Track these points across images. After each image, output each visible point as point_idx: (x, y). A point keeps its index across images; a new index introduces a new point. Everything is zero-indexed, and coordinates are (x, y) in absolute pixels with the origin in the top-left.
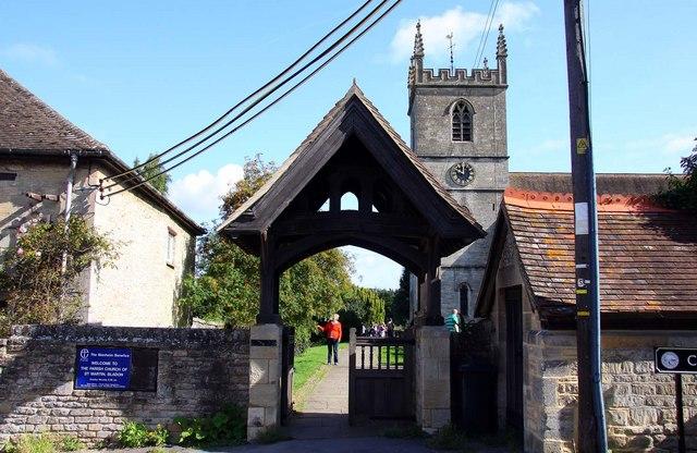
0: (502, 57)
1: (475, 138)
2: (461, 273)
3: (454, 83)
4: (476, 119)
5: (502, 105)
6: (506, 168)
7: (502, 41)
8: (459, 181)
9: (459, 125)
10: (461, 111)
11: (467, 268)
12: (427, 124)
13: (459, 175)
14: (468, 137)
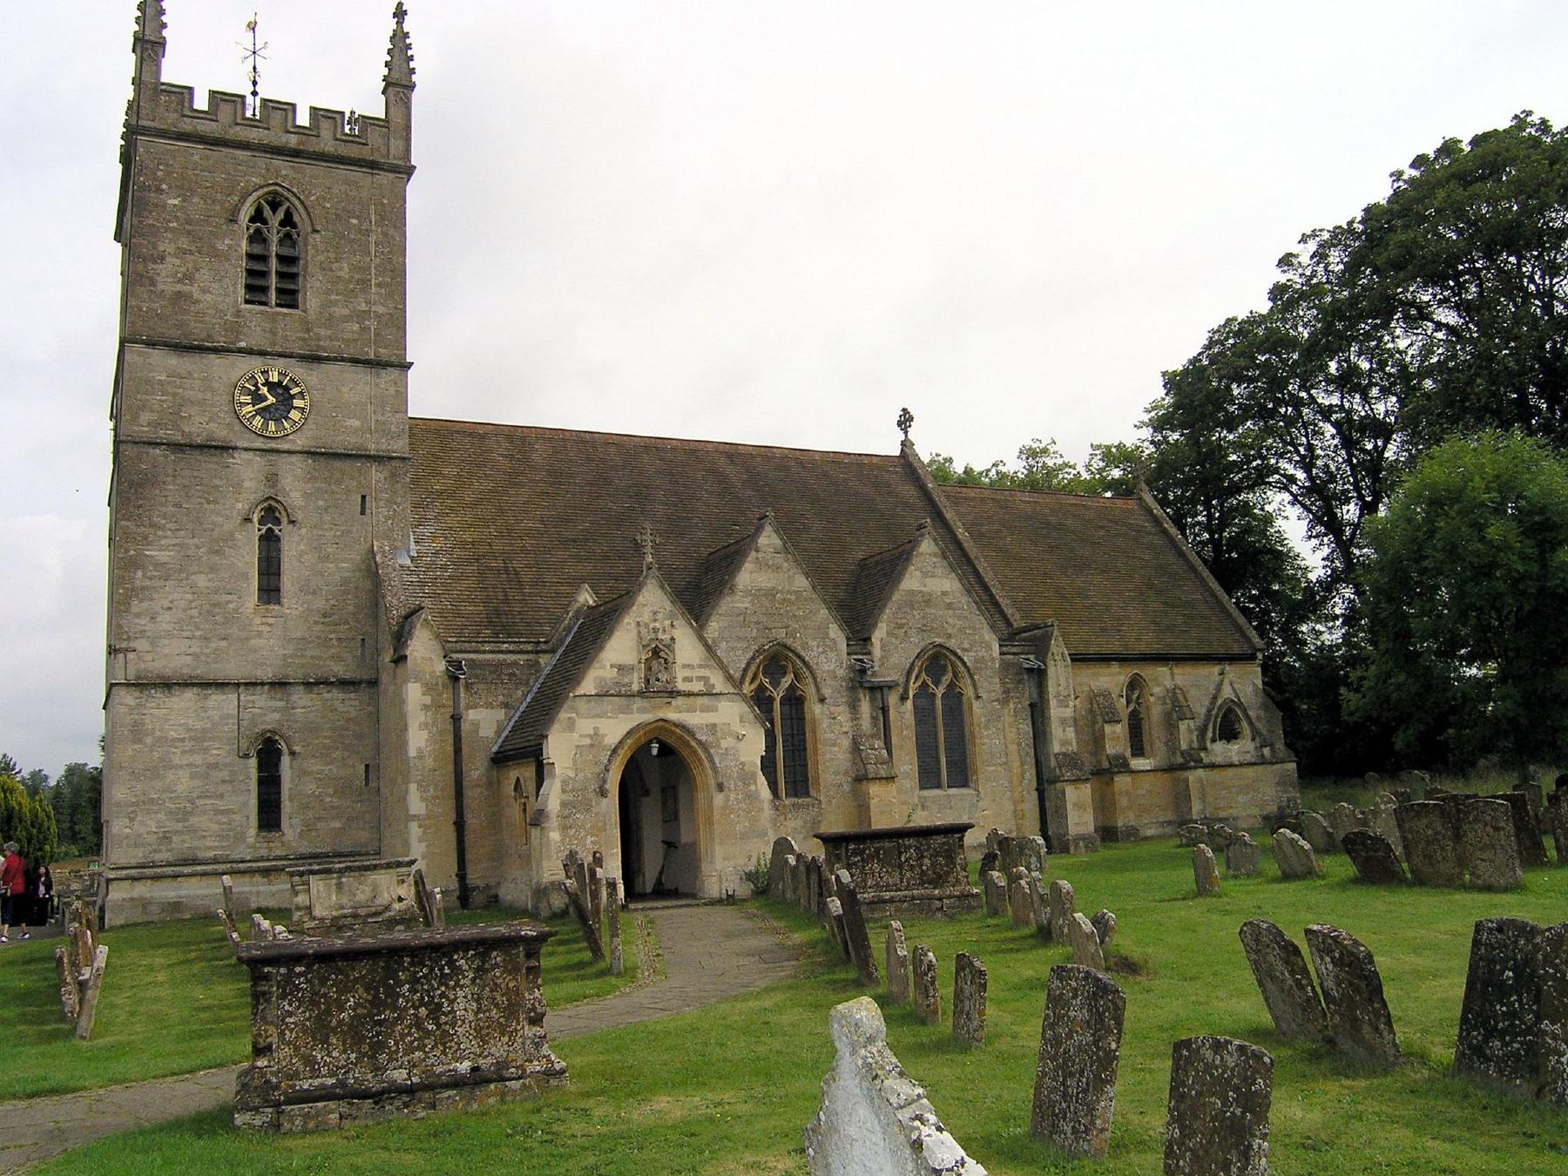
0: (399, 84)
3: (253, 135)
4: (314, 251)
5: (394, 218)
6: (402, 396)
7: (400, 43)
8: (258, 422)
9: (263, 258)
10: (275, 220)
11: (280, 685)
12: (165, 246)
14: (289, 298)
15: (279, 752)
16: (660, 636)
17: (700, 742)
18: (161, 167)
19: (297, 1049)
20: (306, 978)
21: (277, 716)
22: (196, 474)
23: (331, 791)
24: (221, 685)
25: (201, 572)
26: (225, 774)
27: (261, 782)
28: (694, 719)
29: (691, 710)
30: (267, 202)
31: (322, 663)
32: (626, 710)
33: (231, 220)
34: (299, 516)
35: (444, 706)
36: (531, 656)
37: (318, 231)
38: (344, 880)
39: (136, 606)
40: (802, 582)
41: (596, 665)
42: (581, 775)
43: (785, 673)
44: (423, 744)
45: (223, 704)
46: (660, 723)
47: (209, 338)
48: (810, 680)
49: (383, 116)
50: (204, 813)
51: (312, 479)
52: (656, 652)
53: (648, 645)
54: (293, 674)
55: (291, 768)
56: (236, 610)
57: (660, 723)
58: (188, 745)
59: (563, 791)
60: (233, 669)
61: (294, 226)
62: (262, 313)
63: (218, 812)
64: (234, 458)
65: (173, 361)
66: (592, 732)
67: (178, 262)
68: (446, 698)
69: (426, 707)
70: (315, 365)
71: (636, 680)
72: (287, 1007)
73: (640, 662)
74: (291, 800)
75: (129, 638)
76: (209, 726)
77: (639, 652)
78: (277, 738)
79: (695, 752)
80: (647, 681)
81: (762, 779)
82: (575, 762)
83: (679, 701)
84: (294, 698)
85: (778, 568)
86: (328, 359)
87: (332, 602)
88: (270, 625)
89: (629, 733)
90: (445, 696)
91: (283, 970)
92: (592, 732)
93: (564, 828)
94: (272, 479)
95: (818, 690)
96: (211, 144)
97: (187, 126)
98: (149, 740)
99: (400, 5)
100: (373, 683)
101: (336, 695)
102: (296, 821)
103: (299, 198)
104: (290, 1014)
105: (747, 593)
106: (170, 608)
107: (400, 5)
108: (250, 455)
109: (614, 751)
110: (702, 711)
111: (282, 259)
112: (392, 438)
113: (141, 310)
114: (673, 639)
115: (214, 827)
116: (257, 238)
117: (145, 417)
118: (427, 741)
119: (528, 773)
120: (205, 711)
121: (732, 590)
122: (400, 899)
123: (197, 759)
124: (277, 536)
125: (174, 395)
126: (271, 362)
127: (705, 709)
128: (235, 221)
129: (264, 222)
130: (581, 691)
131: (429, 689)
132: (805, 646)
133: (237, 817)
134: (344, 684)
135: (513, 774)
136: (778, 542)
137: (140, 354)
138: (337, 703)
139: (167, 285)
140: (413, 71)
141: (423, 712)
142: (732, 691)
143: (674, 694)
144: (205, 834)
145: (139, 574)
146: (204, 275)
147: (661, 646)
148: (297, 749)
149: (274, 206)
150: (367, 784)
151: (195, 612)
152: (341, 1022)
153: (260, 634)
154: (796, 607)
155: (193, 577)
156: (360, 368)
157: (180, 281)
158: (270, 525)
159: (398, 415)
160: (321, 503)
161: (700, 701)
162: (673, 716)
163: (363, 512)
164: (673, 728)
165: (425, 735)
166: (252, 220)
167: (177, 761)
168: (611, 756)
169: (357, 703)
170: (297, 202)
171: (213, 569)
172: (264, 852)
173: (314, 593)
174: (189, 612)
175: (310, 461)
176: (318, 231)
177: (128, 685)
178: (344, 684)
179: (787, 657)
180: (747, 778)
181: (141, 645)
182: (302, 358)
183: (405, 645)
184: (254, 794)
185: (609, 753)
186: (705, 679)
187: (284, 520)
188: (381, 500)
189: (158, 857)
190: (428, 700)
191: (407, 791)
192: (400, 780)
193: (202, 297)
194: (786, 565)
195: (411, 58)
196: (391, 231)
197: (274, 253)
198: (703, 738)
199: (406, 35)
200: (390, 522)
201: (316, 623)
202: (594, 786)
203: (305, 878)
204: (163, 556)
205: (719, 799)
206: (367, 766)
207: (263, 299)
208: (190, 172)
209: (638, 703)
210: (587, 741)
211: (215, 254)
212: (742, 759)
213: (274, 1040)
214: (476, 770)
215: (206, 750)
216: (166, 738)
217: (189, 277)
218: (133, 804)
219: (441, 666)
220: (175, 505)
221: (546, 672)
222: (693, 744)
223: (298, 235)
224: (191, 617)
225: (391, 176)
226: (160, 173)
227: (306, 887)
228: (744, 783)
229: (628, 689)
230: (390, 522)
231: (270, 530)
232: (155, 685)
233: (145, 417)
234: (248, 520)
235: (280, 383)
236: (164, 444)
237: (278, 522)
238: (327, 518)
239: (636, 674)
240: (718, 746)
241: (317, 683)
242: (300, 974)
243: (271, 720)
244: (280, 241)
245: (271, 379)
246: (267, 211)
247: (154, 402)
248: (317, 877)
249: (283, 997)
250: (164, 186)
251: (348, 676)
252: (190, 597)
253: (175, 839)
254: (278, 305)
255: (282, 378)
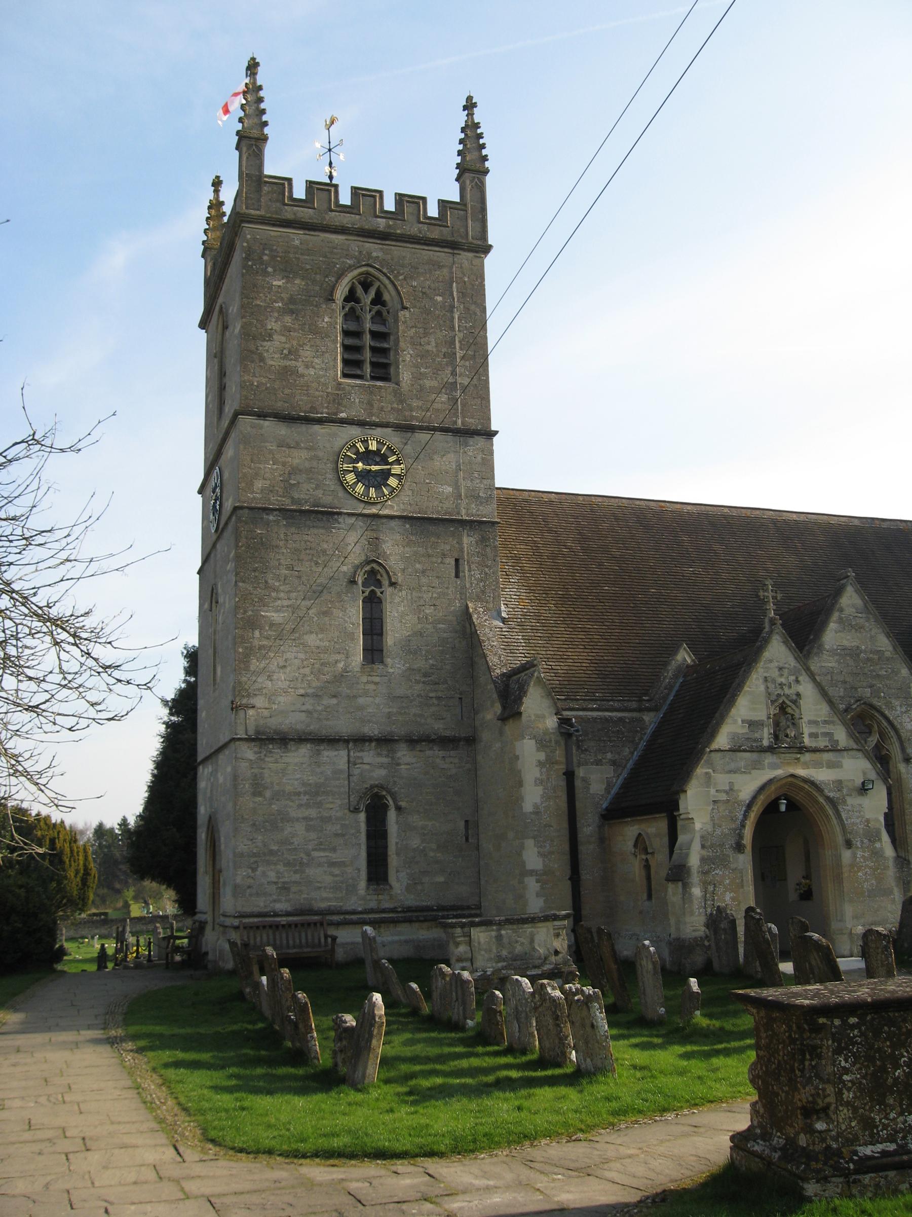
1: (405, 376)
2: (369, 756)
3: (346, 220)
8: (360, 488)
9: (357, 334)
10: (367, 299)
11: (385, 741)
12: (271, 324)
13: (362, 476)
15: (385, 807)
16: (787, 691)
17: (828, 799)
18: (267, 252)
19: (855, 1110)
20: (860, 1031)
21: (383, 772)
22: (306, 538)
23: (434, 846)
24: (332, 741)
25: (312, 633)
26: (337, 828)
27: (369, 836)
28: (822, 775)
29: (818, 765)
30: (360, 283)
31: (423, 721)
32: (756, 766)
33: (330, 300)
34: (399, 578)
35: (557, 763)
36: (635, 714)
37: (406, 308)
38: (503, 932)
39: (254, 664)
40: (884, 643)
41: (729, 720)
42: (718, 832)
43: (870, 733)
44: (538, 800)
45: (338, 758)
46: (790, 779)
47: (313, 409)
48: (894, 739)
49: (457, 199)
50: (320, 865)
51: (409, 544)
52: (783, 708)
53: (776, 701)
54: (398, 730)
55: (397, 822)
56: (345, 670)
57: (790, 779)
58: (304, 799)
59: (703, 847)
60: (343, 725)
61: (384, 304)
62: (360, 386)
63: (332, 864)
64: (339, 523)
65: (282, 430)
66: (727, 788)
67: (283, 339)
68: (559, 755)
69: (540, 764)
70: (409, 434)
71: (766, 735)
72: (843, 1064)
73: (769, 718)
74: (398, 854)
75: (249, 696)
76: (322, 780)
77: (768, 708)
78: (384, 793)
79: (822, 808)
80: (776, 737)
81: (885, 837)
82: (712, 819)
83: (807, 757)
84: (399, 754)
85: (859, 628)
86: (421, 428)
87: (431, 662)
88: (376, 684)
89: (762, 788)
90: (557, 752)
91: (837, 1022)
92: (727, 788)
93: (705, 885)
94: (375, 543)
95: (903, 749)
96: (309, 230)
97: (289, 213)
98: (268, 794)
99: (469, 99)
100: (471, 741)
101: (436, 754)
102: (402, 875)
103: (389, 278)
104: (846, 1071)
105: (833, 652)
106: (285, 667)
107: (469, 99)
108: (352, 520)
109: (749, 806)
110: (829, 767)
111: (375, 335)
112: (481, 503)
113: (253, 384)
114: (798, 695)
115: (329, 879)
116: (351, 315)
117: (259, 484)
118: (542, 797)
119: (655, 828)
120: (319, 766)
121: (821, 647)
122: (557, 953)
123: (312, 813)
124: (379, 598)
125: (284, 464)
126: (370, 432)
127: (831, 765)
128: (333, 300)
129: (358, 301)
130: (715, 746)
131: (542, 744)
132: (891, 708)
133: (349, 870)
134: (445, 742)
135: (630, 831)
136: (858, 602)
137: (253, 426)
138: (438, 760)
139: (274, 361)
140: (485, 158)
141: (538, 769)
142: (855, 746)
143: (802, 749)
144: (319, 885)
145: (257, 633)
146: (307, 353)
147: (788, 702)
148: (403, 804)
149: (366, 286)
150: (467, 839)
151: (307, 671)
152: (896, 1079)
153: (366, 694)
154: (878, 667)
155: (305, 637)
156: (449, 437)
157: (285, 357)
158: (373, 588)
159: (485, 482)
160: (418, 566)
161: (826, 756)
162: (801, 772)
163: (457, 576)
164: (802, 784)
165: (539, 790)
166: (347, 299)
167: (293, 813)
168: (746, 811)
169: (456, 761)
170: (387, 282)
171: (322, 630)
172: (373, 905)
173: (415, 653)
174: (302, 671)
175: (408, 526)
176: (406, 308)
177: (249, 740)
178: (445, 742)
179: (872, 717)
180: (873, 836)
181: (259, 702)
182: (399, 428)
183: (519, 700)
184: (364, 848)
185: (744, 809)
186: (829, 735)
187: (385, 582)
188: (472, 563)
189: (280, 907)
190: (542, 756)
191: (522, 847)
192: (511, 835)
193: (306, 372)
194: (867, 624)
195: (483, 146)
196: (473, 307)
197: (368, 329)
198: (831, 795)
199: (477, 126)
200: (482, 584)
201: (417, 682)
202: (732, 841)
203: (466, 930)
204: (276, 617)
205: (846, 855)
206: (467, 821)
207: (359, 372)
208: (291, 256)
209: (769, 759)
210: (723, 797)
211: (315, 331)
212: (868, 816)
213: (831, 1099)
214: (588, 828)
215: (319, 805)
216: (284, 791)
217: (293, 353)
218: (255, 855)
219: (551, 722)
220: (288, 568)
221: (649, 731)
222: (821, 800)
223: (388, 313)
224: (305, 675)
225: (470, 255)
226: (265, 258)
227: (467, 939)
228: (870, 840)
229: (759, 744)
230: (482, 584)
231: (373, 592)
232: (271, 740)
233: (259, 484)
234: (353, 582)
235: (379, 450)
236: (275, 510)
237: (379, 584)
238: (424, 580)
239: (766, 730)
240: (844, 802)
241: (419, 741)
242: (853, 1027)
243: (379, 775)
244: (372, 318)
245: (370, 448)
246: (359, 290)
247: (267, 470)
248: (478, 929)
249: (838, 1051)
250: (270, 269)
251: (448, 733)
252: (301, 656)
253: (294, 889)
254: (373, 378)
255: (380, 446)
